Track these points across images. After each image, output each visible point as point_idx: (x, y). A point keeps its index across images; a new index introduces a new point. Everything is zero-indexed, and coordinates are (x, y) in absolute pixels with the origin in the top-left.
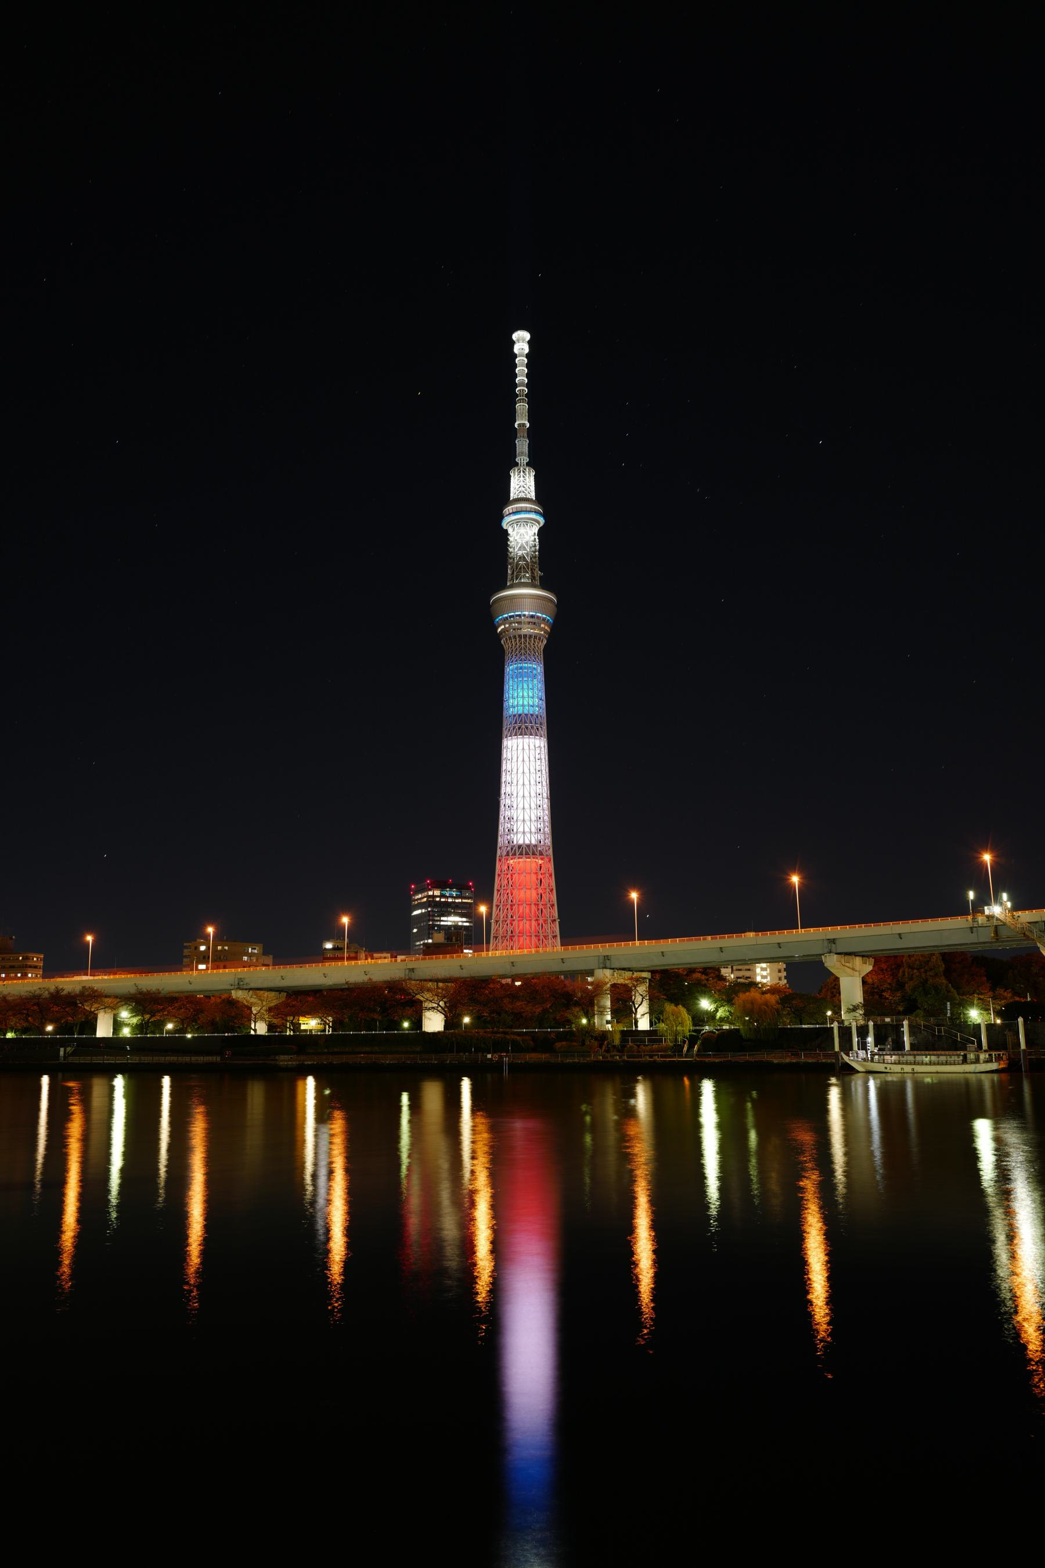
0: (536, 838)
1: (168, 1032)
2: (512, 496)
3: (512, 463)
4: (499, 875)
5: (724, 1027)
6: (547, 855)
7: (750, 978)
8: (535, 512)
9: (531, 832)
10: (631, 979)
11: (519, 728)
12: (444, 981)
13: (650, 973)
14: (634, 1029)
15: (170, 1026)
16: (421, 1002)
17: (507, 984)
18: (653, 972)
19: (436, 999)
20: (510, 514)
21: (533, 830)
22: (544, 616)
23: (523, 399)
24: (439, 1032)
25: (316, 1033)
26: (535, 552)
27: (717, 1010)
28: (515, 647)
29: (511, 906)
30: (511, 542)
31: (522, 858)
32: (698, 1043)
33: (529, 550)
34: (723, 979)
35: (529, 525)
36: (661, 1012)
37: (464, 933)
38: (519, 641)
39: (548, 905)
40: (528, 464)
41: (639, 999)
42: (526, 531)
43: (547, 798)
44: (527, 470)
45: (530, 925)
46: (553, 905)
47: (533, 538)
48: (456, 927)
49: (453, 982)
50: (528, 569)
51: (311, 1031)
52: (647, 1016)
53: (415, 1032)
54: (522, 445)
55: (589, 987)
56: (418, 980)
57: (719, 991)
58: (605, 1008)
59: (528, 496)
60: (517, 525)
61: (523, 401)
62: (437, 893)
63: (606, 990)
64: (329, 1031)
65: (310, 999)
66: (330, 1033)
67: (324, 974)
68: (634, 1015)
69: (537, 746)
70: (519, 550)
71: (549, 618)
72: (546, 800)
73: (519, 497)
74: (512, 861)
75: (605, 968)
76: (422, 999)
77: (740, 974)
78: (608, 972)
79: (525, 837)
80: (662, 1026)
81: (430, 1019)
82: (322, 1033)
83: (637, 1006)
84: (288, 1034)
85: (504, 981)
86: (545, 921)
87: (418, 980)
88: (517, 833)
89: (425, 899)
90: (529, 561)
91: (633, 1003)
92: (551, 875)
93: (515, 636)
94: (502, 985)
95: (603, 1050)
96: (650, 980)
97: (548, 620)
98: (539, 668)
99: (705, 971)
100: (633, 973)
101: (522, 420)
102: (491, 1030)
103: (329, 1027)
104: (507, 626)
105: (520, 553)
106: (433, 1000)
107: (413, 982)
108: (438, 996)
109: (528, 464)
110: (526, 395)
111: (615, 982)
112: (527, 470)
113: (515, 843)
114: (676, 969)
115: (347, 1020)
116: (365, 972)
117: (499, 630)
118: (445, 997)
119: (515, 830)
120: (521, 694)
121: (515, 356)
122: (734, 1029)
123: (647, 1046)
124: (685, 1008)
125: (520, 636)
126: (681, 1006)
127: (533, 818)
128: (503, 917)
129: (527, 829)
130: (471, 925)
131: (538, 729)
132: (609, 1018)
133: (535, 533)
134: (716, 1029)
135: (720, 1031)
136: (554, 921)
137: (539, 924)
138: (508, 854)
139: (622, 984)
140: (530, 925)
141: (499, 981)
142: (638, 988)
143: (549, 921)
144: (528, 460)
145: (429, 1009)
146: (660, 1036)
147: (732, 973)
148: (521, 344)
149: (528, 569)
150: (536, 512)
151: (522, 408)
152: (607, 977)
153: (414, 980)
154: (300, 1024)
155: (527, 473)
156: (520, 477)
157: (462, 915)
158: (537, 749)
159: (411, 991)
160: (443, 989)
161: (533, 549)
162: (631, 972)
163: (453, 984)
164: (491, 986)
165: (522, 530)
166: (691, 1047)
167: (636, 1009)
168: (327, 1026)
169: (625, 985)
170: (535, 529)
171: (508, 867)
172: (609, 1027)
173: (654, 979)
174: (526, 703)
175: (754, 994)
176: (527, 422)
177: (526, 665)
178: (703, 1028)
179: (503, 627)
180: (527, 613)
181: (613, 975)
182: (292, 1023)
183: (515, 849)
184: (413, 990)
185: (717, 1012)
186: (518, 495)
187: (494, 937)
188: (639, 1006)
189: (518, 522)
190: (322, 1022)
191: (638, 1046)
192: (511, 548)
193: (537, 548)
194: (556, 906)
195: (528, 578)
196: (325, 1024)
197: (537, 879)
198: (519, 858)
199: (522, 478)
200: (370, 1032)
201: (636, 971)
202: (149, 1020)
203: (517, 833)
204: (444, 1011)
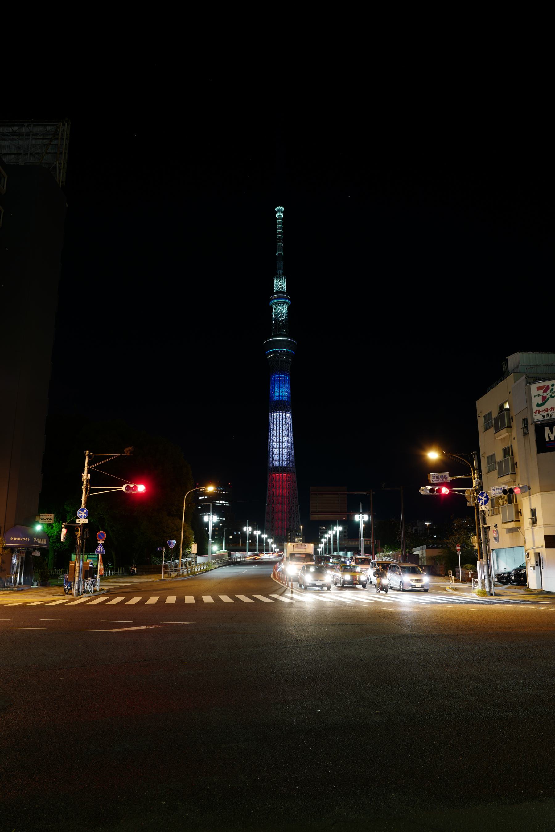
11: (281, 408)
31: (278, 473)
35: (284, 305)
54: (280, 264)
69: (289, 417)
70: (280, 317)
71: (293, 352)
110: (282, 239)
113: (275, 465)
117: (268, 358)
120: (281, 390)
131: (287, 408)
151: (280, 244)
156: (280, 280)
165: (281, 308)
176: (283, 253)
183: (275, 469)
189: (279, 303)
199: (281, 281)
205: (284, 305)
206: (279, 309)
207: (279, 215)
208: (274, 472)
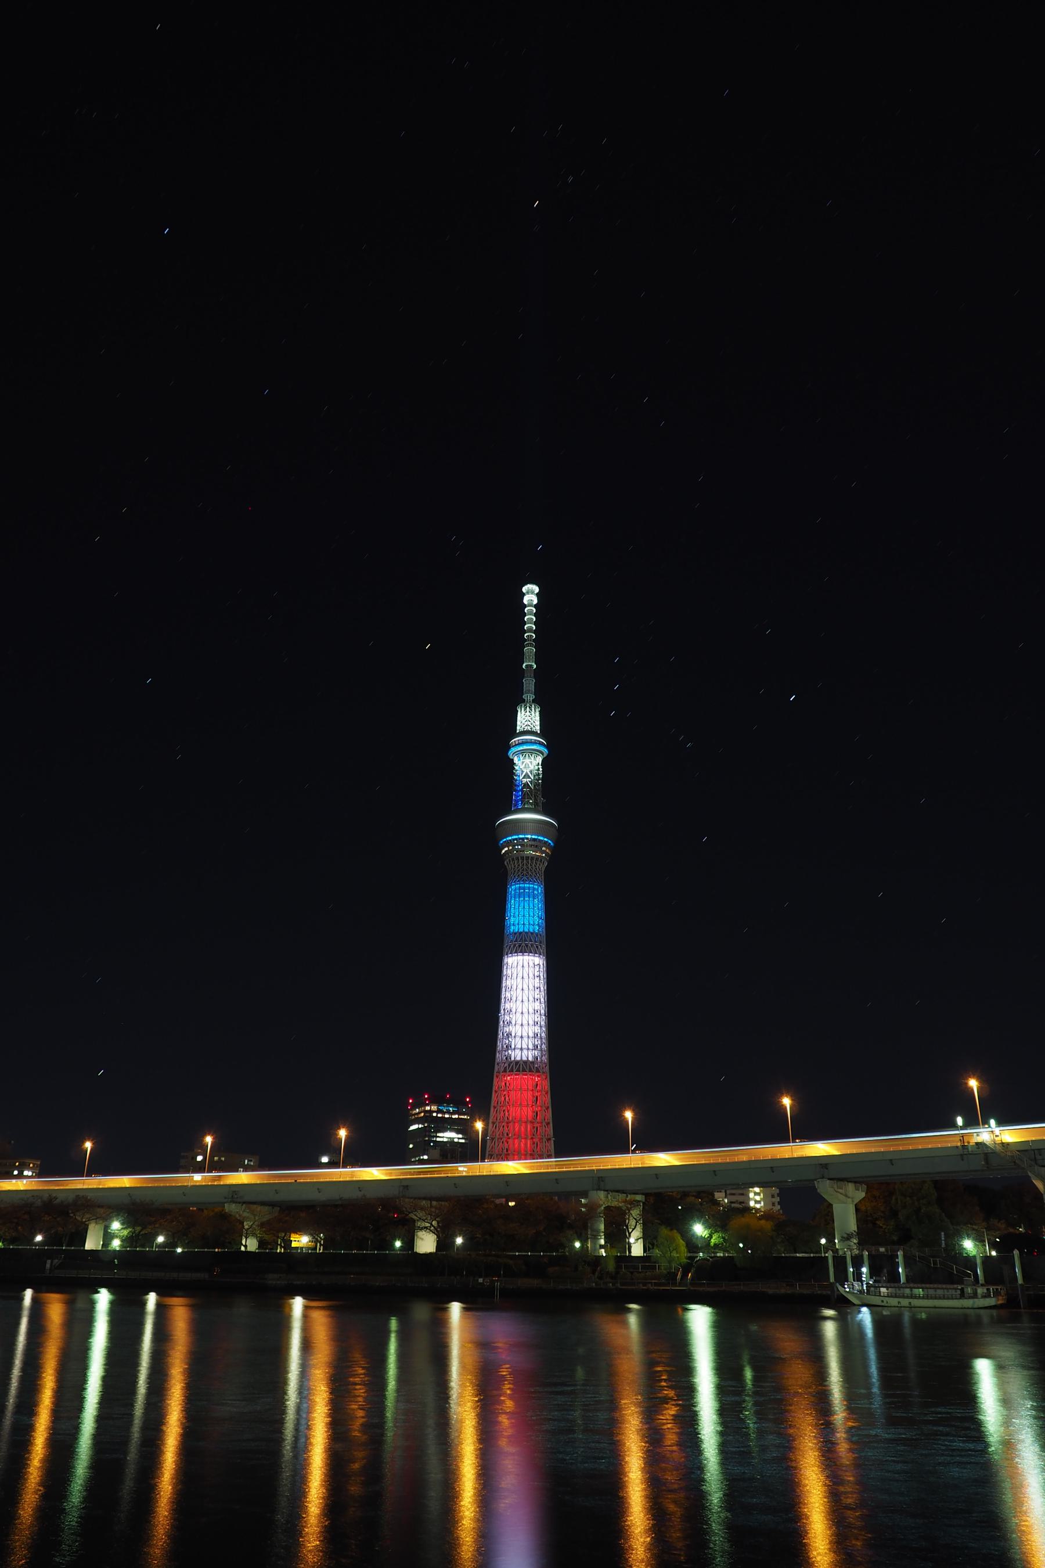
0: (533, 1055)
1: (159, 1246)
2: (519, 729)
3: (517, 701)
4: (496, 1092)
5: (718, 1255)
6: (543, 1073)
7: (743, 1203)
8: (539, 744)
9: (528, 1049)
10: (625, 1201)
11: (520, 946)
12: (438, 1199)
13: (644, 1196)
14: (627, 1255)
15: (161, 1239)
16: (414, 1221)
17: (502, 1204)
18: (647, 1195)
19: (429, 1218)
20: (516, 745)
21: (531, 1047)
22: (546, 839)
23: (531, 644)
24: (431, 1253)
25: (307, 1251)
26: (538, 780)
27: (711, 1237)
28: (518, 868)
29: (507, 1123)
30: (516, 771)
31: (518, 1075)
32: (692, 1271)
33: (532, 778)
34: (717, 1203)
36: (655, 1238)
37: (460, 1149)
38: (522, 863)
39: (544, 1124)
40: (534, 701)
41: (633, 1222)
42: (530, 760)
43: (545, 1015)
44: (533, 706)
45: (526, 1144)
46: (548, 1124)
47: (537, 767)
48: (451, 1142)
49: (446, 1201)
50: (532, 795)
51: (302, 1248)
52: (641, 1241)
53: (407, 1252)
54: (529, 684)
55: (583, 1209)
56: (411, 1198)
57: (713, 1216)
58: (598, 1231)
59: (534, 729)
60: (522, 755)
61: (531, 645)
62: (434, 1108)
63: (600, 1213)
64: (320, 1250)
65: (303, 1215)
66: (321, 1251)
67: (318, 1189)
68: (627, 1240)
69: (536, 964)
71: (550, 841)
72: (544, 1017)
73: (525, 730)
74: (509, 1078)
75: (599, 1189)
76: (415, 1217)
77: (734, 1198)
78: (602, 1194)
79: (523, 1053)
80: (657, 1252)
81: (422, 1239)
82: (313, 1251)
83: (630, 1230)
84: (278, 1251)
85: (498, 1201)
86: (541, 1139)
87: (411, 1198)
88: (514, 1049)
89: (422, 1114)
90: (533, 788)
91: (627, 1227)
92: (547, 1093)
93: (518, 858)
94: (496, 1206)
95: (596, 1276)
96: (644, 1203)
97: (550, 843)
98: (539, 889)
99: (699, 1195)
100: (627, 1196)
101: (529, 663)
102: (483, 1252)
103: (321, 1245)
104: (511, 848)
105: (525, 780)
106: (426, 1219)
107: (407, 1200)
108: (431, 1215)
109: (534, 701)
111: (609, 1204)
112: (533, 706)
113: (513, 1059)
114: (670, 1192)
115: (339, 1238)
116: (359, 1188)
117: (503, 851)
118: (438, 1217)
119: (513, 1047)
120: (522, 913)
121: (525, 606)
122: (728, 1256)
123: (642, 1272)
124: (680, 1233)
125: (522, 858)
126: (675, 1231)
127: (531, 1034)
128: (499, 1135)
129: (524, 1046)
130: (467, 1142)
132: (602, 1242)
133: (539, 763)
134: (710, 1257)
135: (714, 1259)
136: (549, 1140)
137: (534, 1143)
138: (505, 1071)
139: (616, 1207)
140: (526, 1144)
141: (493, 1201)
142: (631, 1212)
143: (544, 1140)
144: (534, 697)
145: (421, 1229)
146: (655, 1263)
147: (725, 1198)
148: (530, 595)
149: (532, 795)
150: (540, 743)
151: (530, 650)
152: (601, 1200)
153: (408, 1198)
154: (292, 1241)
155: (533, 709)
157: (458, 1132)
158: (536, 967)
159: (404, 1209)
160: (436, 1208)
161: (537, 777)
162: (625, 1195)
163: (446, 1203)
164: (485, 1206)
165: (527, 761)
166: (685, 1275)
167: (630, 1234)
168: (318, 1244)
169: (618, 1208)
170: (539, 759)
171: (505, 1084)
172: (603, 1252)
173: (648, 1202)
174: (526, 922)
175: (744, 1220)
176: (533, 664)
177: (528, 885)
178: (696, 1255)
179: (506, 849)
180: (529, 836)
181: (607, 1197)
182: (283, 1240)
183: (513, 1066)
184: (406, 1208)
185: (710, 1239)
186: (524, 728)
187: (489, 1155)
188: (633, 1229)
189: (523, 752)
190: (314, 1240)
191: (632, 1273)
192: (516, 776)
193: (541, 776)
194: (551, 1125)
195: (531, 804)
196: (316, 1241)
197: (534, 1097)
198: (516, 1075)
199: (528, 713)
200: (361, 1252)
201: (630, 1194)
202: (140, 1232)
203: (514, 1049)
204: (437, 1231)
205: (532, 755)
206: (523, 762)
207: (529, 599)
208: (512, 1073)
